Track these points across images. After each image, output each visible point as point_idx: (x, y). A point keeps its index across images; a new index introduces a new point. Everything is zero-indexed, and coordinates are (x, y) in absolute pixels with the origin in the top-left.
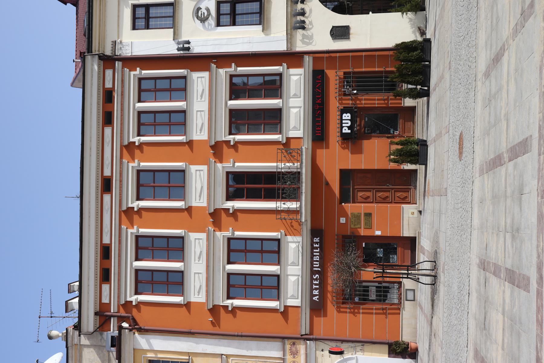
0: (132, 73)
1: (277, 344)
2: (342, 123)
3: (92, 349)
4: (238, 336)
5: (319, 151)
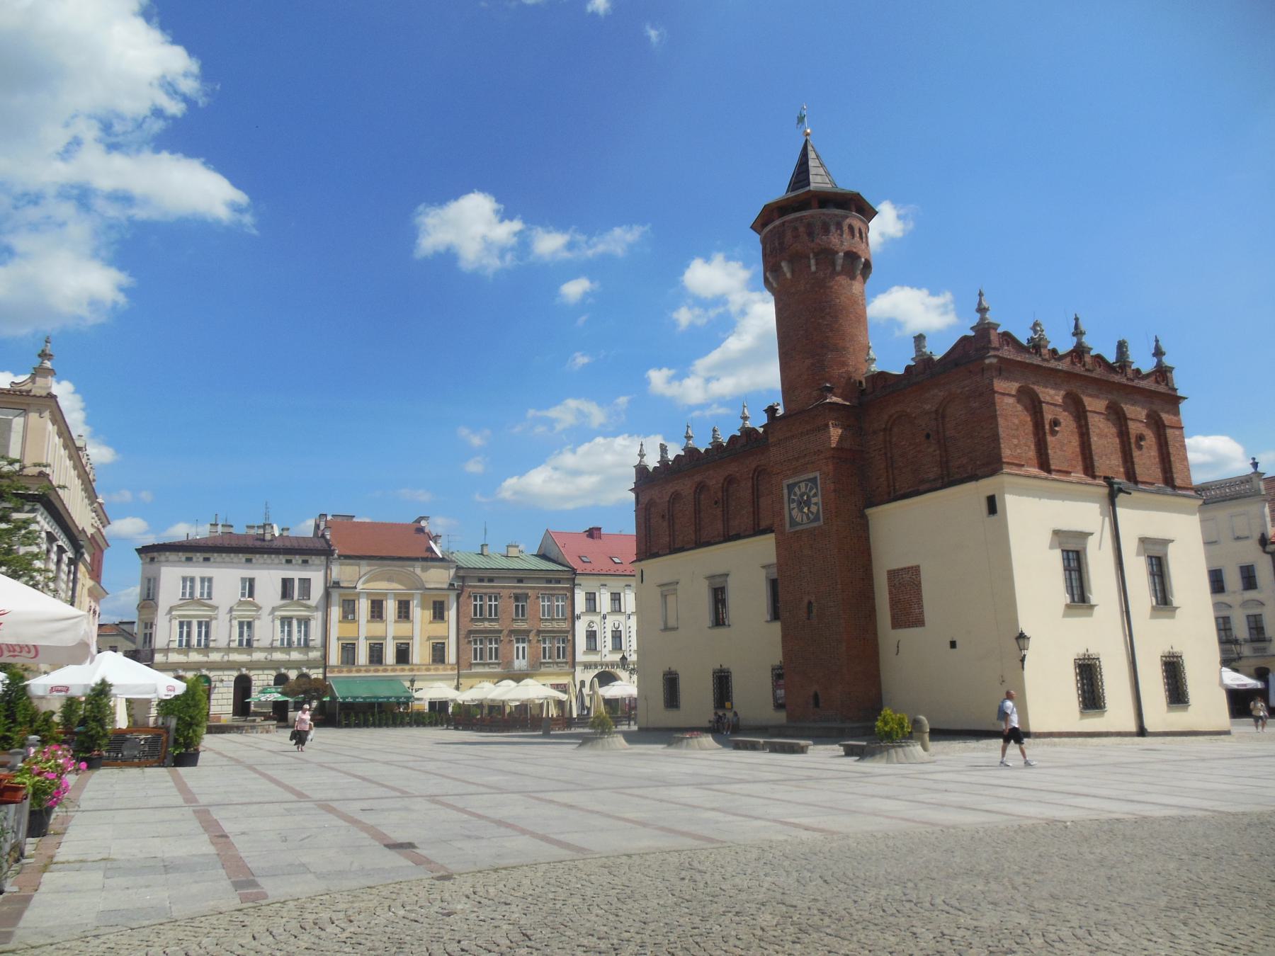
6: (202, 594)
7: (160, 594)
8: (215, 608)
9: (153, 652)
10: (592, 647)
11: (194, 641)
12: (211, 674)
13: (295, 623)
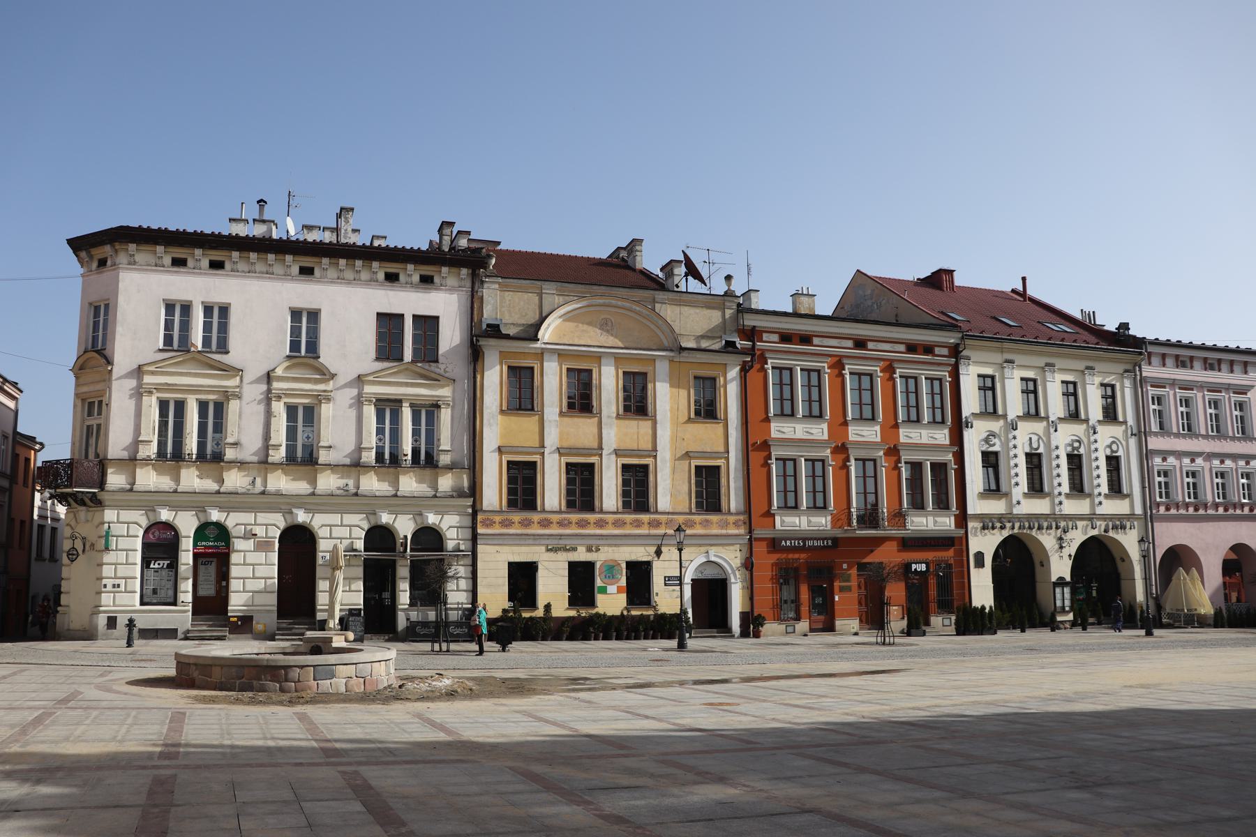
0: (947, 374)
1: (742, 508)
2: (919, 563)
3: (721, 320)
4: (748, 470)
5: (895, 543)
6: (207, 341)
7: (118, 337)
8: (236, 371)
9: (102, 464)
10: (994, 490)
11: (191, 444)
12: (234, 521)
13: (407, 414)
